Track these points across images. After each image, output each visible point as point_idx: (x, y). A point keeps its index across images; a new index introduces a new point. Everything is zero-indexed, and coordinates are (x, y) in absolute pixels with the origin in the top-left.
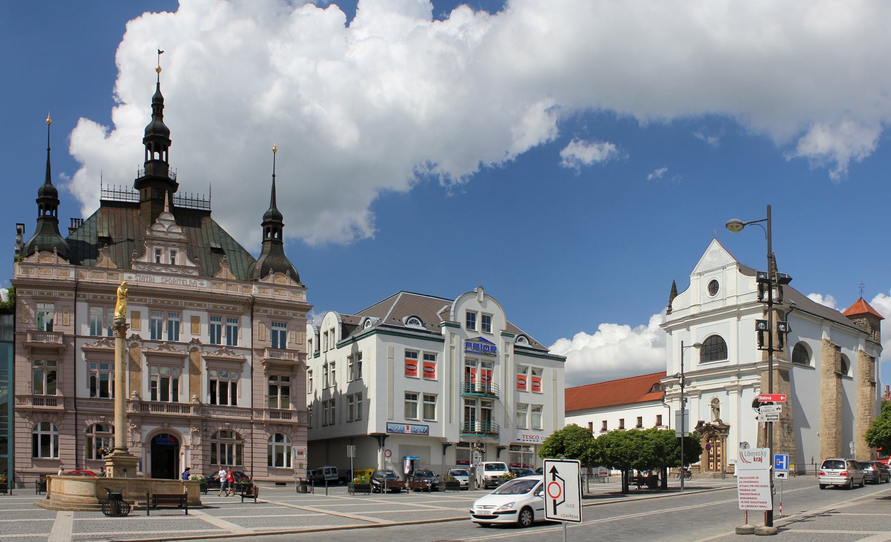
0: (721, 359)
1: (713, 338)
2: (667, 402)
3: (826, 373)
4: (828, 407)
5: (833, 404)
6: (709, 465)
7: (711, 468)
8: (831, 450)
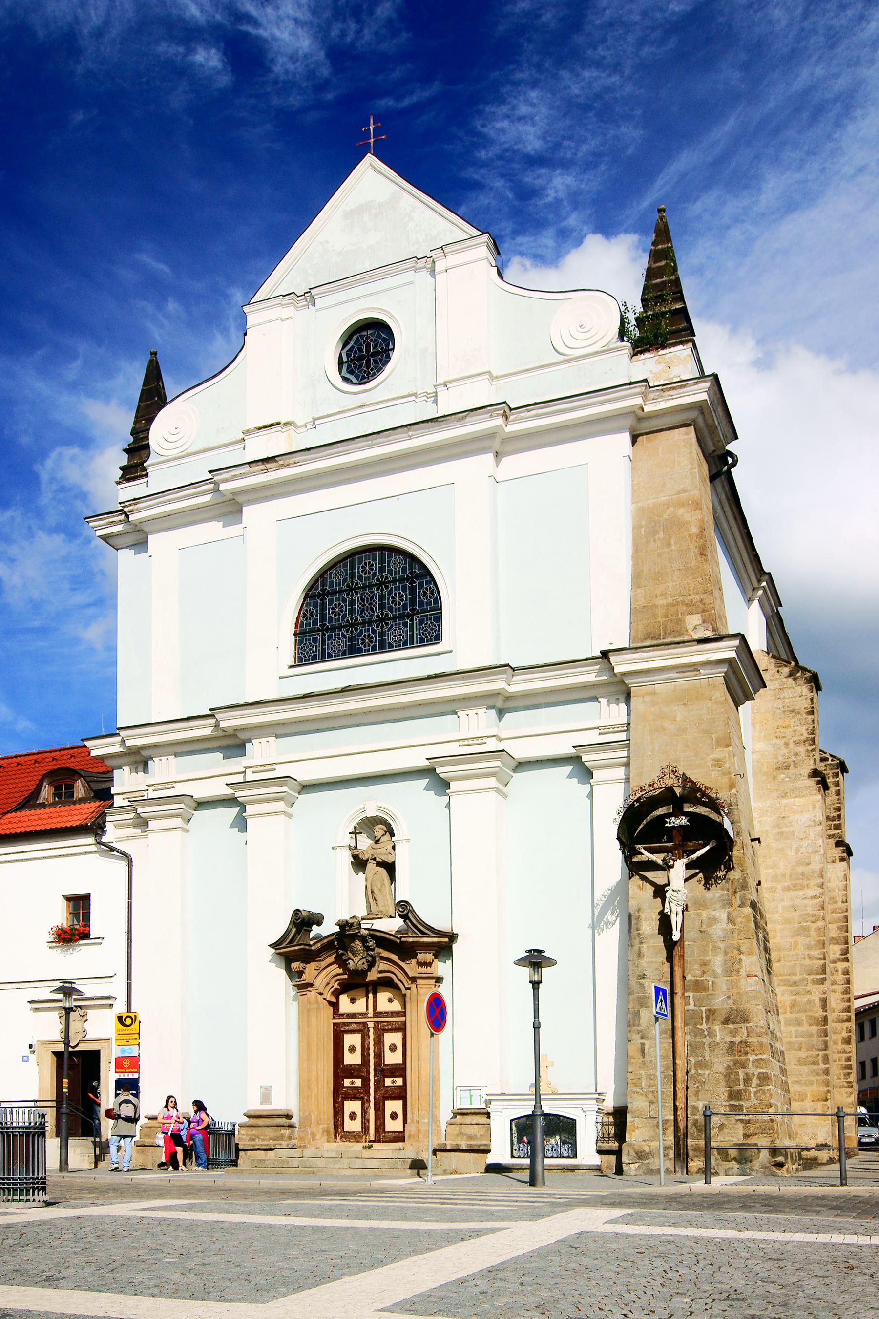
0: (422, 642)
1: (367, 559)
2: (120, 840)
3: (774, 778)
4: (787, 903)
5: (811, 893)
6: (338, 1112)
7: (352, 1126)
8: (805, 1069)
